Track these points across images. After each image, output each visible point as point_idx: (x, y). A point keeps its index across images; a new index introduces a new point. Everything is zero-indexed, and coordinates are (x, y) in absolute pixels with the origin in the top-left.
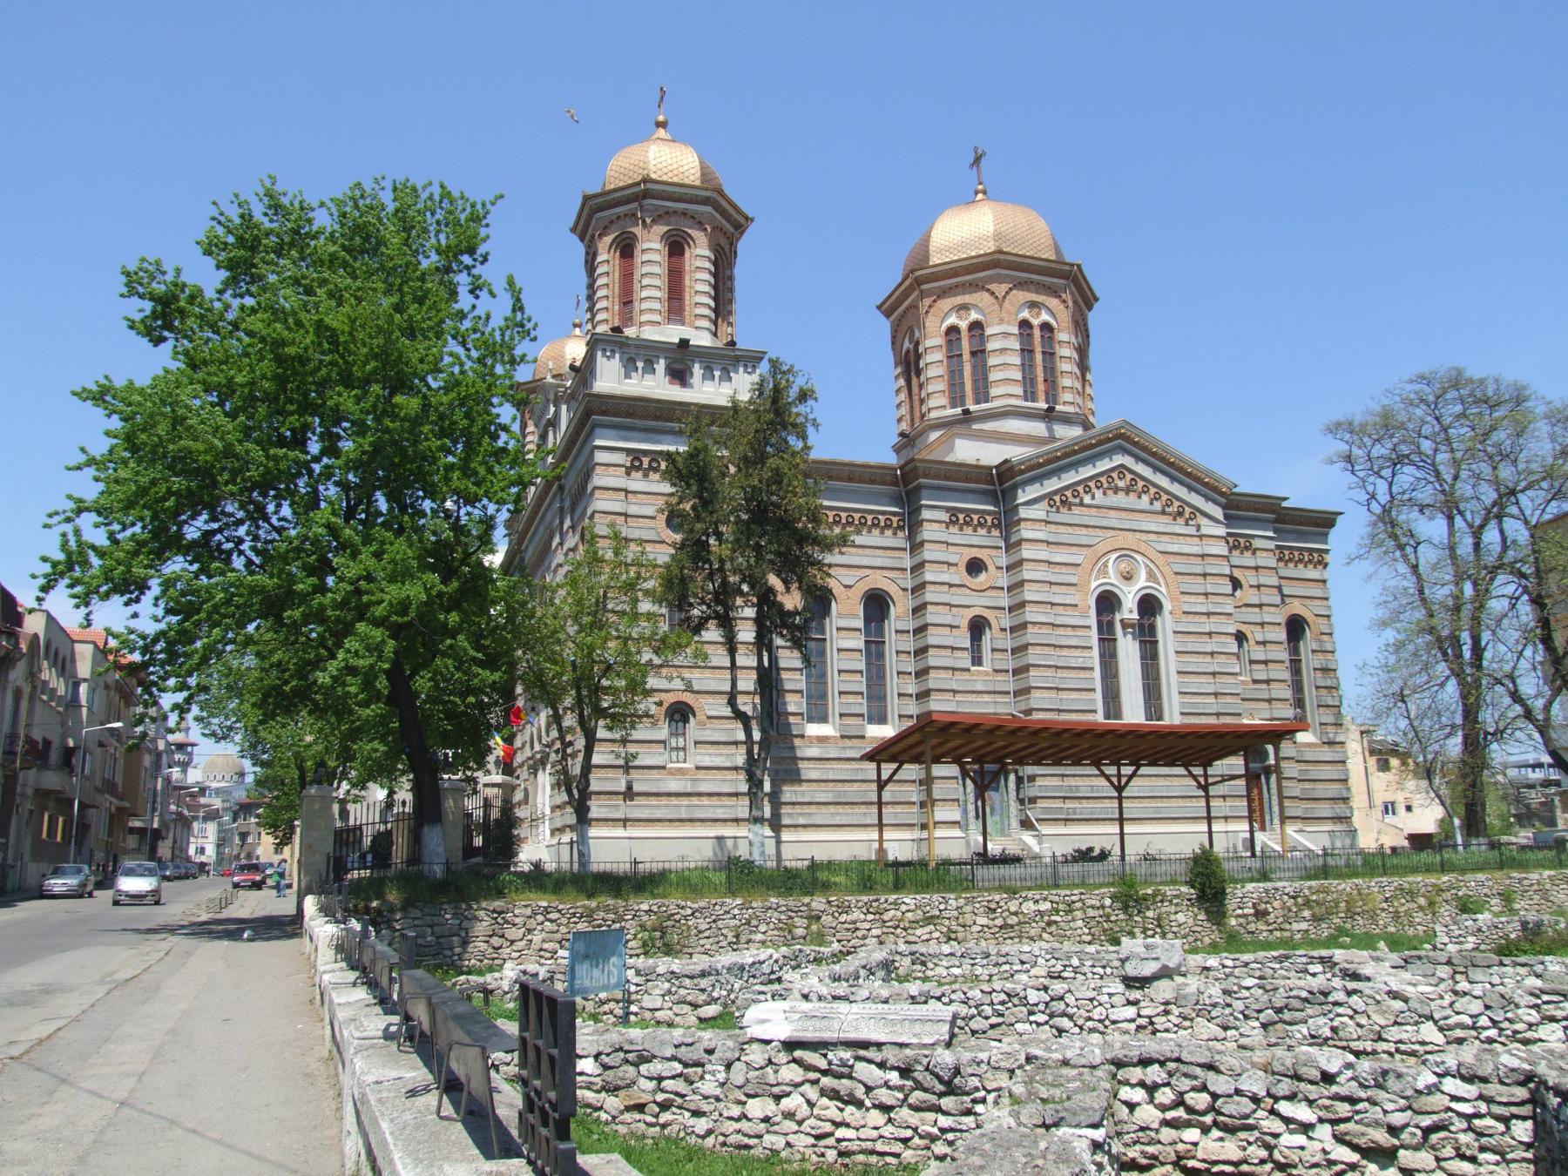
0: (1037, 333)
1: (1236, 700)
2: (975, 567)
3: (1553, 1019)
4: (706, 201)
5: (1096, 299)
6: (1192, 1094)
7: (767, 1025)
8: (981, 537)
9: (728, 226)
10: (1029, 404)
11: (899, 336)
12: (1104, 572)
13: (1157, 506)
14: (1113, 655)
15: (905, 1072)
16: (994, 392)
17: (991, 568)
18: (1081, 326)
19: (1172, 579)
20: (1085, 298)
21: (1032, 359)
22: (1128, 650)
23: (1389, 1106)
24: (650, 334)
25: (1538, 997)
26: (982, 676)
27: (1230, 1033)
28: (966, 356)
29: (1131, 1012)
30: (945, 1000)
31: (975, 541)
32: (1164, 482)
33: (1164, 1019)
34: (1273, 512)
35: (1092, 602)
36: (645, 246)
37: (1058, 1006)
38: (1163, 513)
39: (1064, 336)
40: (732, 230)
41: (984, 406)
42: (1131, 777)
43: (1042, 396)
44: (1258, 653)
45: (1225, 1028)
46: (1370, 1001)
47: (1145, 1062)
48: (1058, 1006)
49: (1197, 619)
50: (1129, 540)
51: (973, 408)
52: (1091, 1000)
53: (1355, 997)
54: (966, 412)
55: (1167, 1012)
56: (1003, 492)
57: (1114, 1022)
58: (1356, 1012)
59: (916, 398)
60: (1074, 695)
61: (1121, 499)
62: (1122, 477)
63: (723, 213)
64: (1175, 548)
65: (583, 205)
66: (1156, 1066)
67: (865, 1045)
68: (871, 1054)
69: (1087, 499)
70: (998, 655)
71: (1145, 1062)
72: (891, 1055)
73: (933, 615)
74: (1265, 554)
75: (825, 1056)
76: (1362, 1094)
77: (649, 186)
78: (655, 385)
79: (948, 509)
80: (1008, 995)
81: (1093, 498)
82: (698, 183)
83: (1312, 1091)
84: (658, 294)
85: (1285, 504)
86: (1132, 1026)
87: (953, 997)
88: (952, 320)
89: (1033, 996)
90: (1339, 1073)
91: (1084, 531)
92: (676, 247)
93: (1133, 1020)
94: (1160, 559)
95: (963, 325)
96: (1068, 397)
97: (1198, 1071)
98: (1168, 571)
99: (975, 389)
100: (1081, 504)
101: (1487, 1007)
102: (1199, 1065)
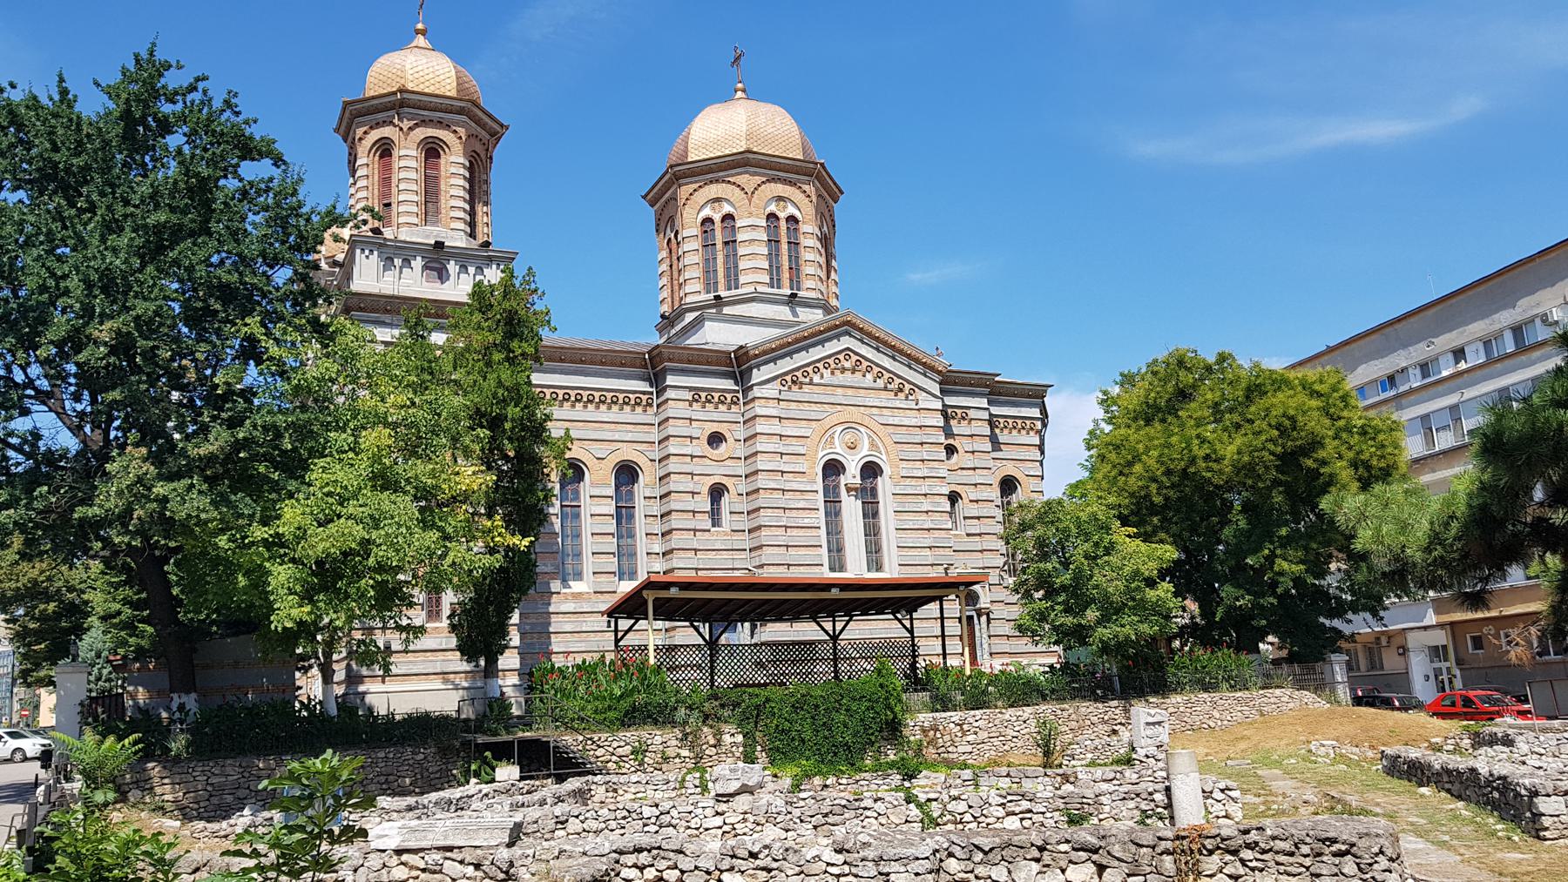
0: (783, 224)
1: (948, 552)
2: (716, 439)
3: (1014, 814)
4: (460, 111)
5: (842, 193)
6: (668, 871)
7: (385, 839)
8: (722, 413)
9: (483, 133)
10: (775, 291)
11: (662, 228)
13: (880, 383)
14: (838, 513)
15: (477, 866)
16: (742, 279)
17: (730, 440)
18: (826, 217)
19: (892, 447)
20: (829, 192)
21: (778, 250)
22: (852, 509)
23: (790, 872)
24: (405, 235)
25: (1005, 797)
26: (718, 537)
27: (790, 834)
28: (719, 246)
29: (718, 821)
30: (581, 818)
31: (715, 416)
32: (887, 362)
33: (743, 825)
34: (987, 386)
36: (402, 153)
37: (665, 819)
38: (885, 389)
39: (809, 227)
40: (488, 137)
41: (734, 292)
42: (848, 622)
43: (786, 282)
44: (974, 510)
45: (787, 831)
46: (889, 806)
47: (639, 850)
48: (665, 819)
49: (913, 482)
50: (854, 414)
51: (723, 294)
52: (690, 813)
53: (879, 803)
54: (718, 298)
55: (745, 820)
56: (741, 373)
57: (707, 829)
58: (880, 815)
59: (675, 282)
60: (803, 551)
61: (848, 378)
63: (478, 122)
65: (344, 109)
66: (646, 852)
67: (450, 849)
68: (455, 855)
70: (735, 517)
71: (639, 850)
72: (468, 856)
73: (675, 483)
74: (980, 423)
75: (423, 858)
76: (775, 865)
77: (405, 96)
78: (413, 283)
79: (690, 389)
80: (629, 812)
81: (822, 377)
82: (453, 93)
83: (743, 865)
84: (415, 198)
85: (997, 379)
86: (720, 832)
87: (588, 815)
88: (707, 212)
89: (647, 811)
90: (760, 852)
91: (814, 407)
92: (432, 151)
93: (720, 827)
94: (882, 431)
95: (717, 218)
96: (810, 283)
97: (672, 855)
98: (888, 441)
99: (727, 276)
100: (811, 383)
101: (970, 807)
102: (673, 851)
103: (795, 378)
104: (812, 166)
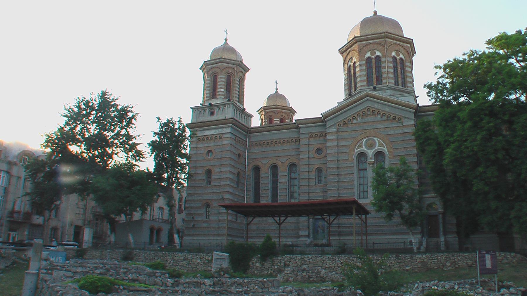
0: (374, 61)
12: (361, 146)
13: (384, 118)
32: (387, 109)
35: (355, 157)
38: (388, 120)
61: (369, 119)
62: (368, 110)
64: (392, 133)
69: (355, 121)
81: (357, 120)
103: (345, 123)
104: (383, 34)
